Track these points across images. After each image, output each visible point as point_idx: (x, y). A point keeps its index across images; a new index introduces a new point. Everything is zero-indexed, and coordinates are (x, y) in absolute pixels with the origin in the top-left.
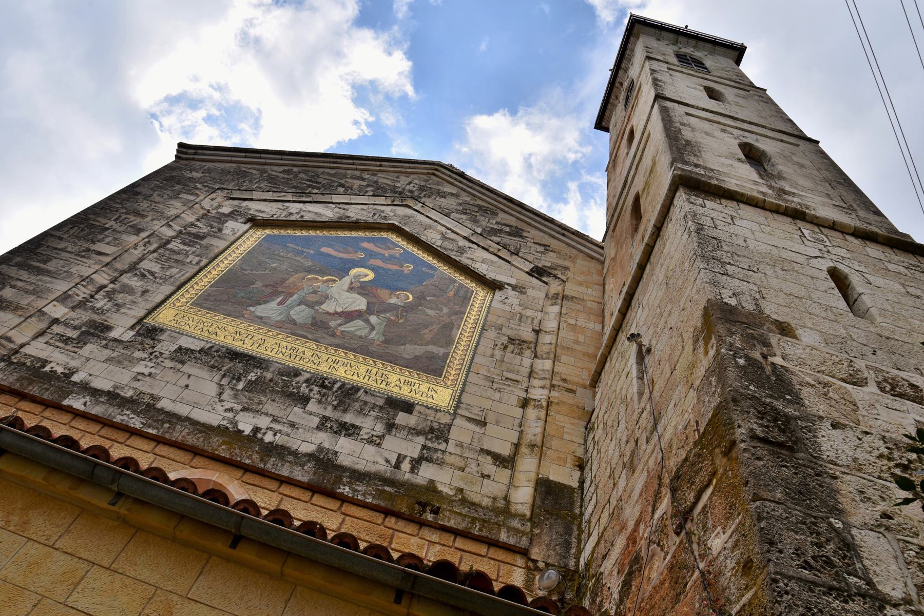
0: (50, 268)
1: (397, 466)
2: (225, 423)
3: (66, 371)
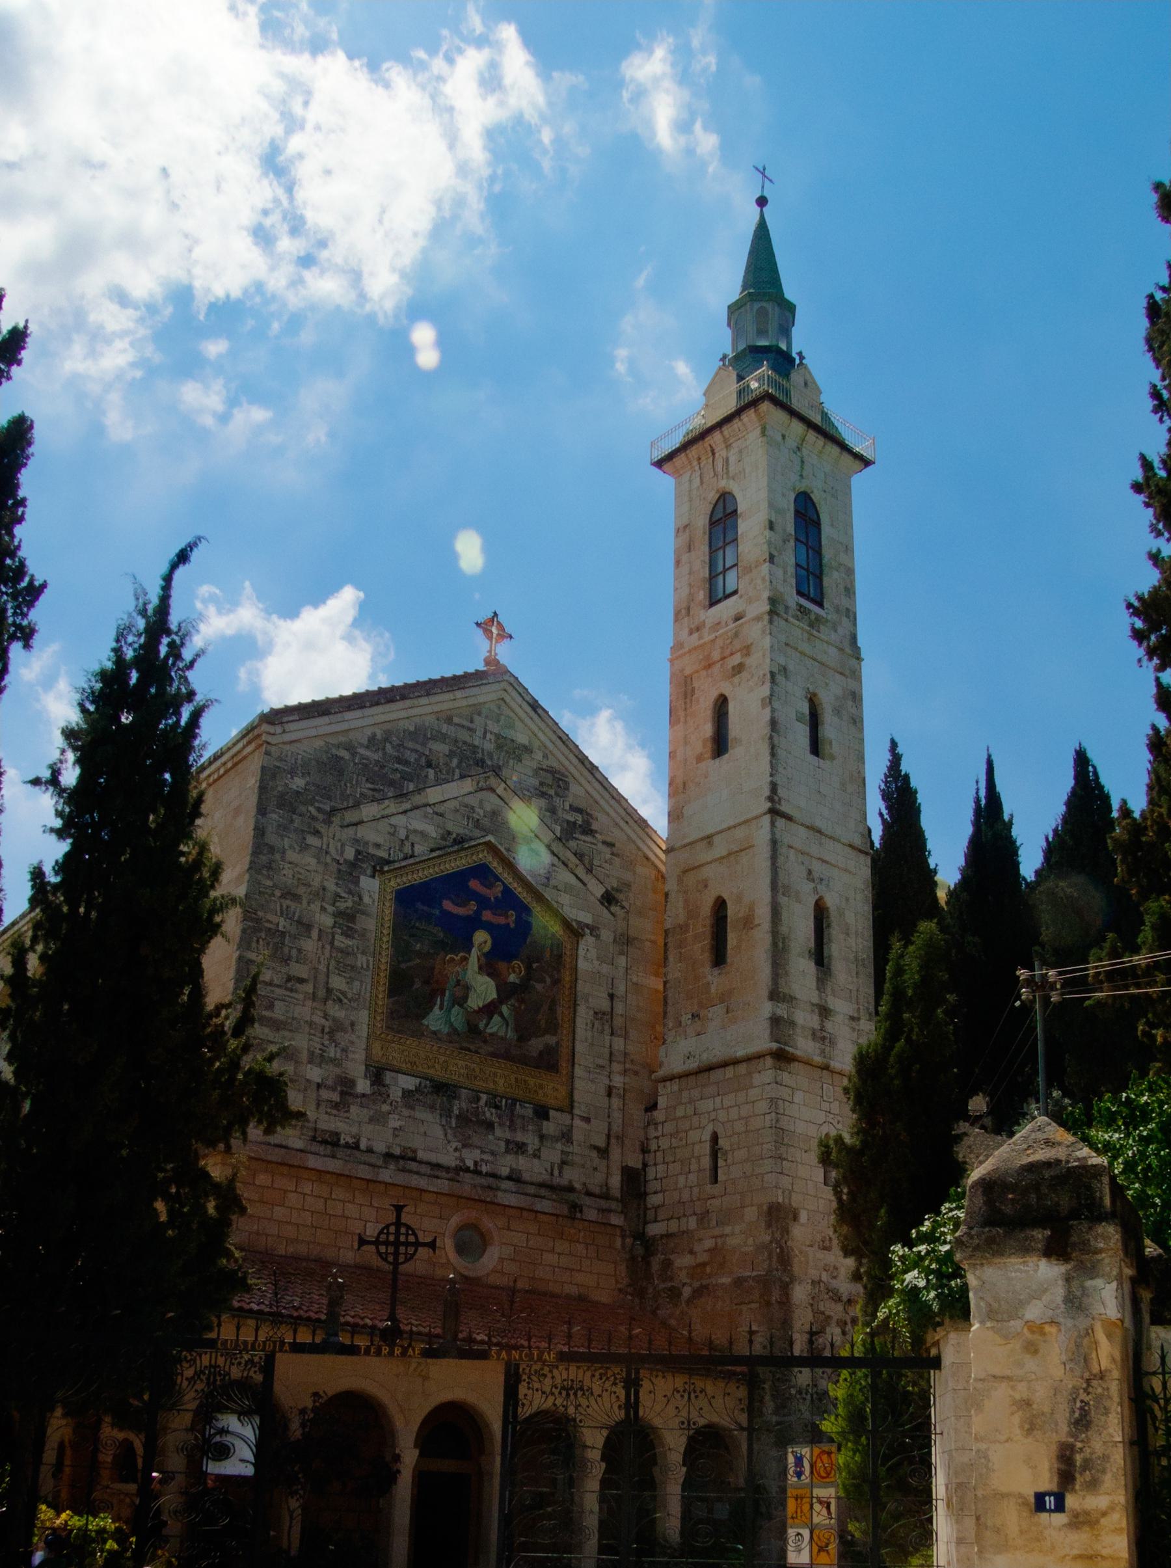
0: (282, 1018)
1: (552, 1174)
2: (458, 1162)
3: (354, 1140)
